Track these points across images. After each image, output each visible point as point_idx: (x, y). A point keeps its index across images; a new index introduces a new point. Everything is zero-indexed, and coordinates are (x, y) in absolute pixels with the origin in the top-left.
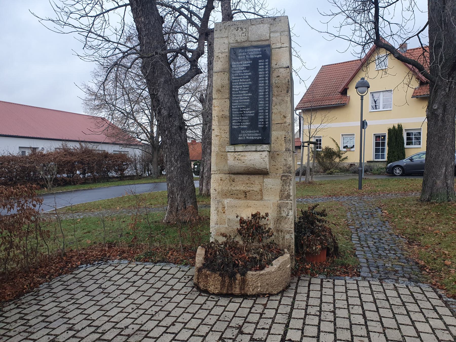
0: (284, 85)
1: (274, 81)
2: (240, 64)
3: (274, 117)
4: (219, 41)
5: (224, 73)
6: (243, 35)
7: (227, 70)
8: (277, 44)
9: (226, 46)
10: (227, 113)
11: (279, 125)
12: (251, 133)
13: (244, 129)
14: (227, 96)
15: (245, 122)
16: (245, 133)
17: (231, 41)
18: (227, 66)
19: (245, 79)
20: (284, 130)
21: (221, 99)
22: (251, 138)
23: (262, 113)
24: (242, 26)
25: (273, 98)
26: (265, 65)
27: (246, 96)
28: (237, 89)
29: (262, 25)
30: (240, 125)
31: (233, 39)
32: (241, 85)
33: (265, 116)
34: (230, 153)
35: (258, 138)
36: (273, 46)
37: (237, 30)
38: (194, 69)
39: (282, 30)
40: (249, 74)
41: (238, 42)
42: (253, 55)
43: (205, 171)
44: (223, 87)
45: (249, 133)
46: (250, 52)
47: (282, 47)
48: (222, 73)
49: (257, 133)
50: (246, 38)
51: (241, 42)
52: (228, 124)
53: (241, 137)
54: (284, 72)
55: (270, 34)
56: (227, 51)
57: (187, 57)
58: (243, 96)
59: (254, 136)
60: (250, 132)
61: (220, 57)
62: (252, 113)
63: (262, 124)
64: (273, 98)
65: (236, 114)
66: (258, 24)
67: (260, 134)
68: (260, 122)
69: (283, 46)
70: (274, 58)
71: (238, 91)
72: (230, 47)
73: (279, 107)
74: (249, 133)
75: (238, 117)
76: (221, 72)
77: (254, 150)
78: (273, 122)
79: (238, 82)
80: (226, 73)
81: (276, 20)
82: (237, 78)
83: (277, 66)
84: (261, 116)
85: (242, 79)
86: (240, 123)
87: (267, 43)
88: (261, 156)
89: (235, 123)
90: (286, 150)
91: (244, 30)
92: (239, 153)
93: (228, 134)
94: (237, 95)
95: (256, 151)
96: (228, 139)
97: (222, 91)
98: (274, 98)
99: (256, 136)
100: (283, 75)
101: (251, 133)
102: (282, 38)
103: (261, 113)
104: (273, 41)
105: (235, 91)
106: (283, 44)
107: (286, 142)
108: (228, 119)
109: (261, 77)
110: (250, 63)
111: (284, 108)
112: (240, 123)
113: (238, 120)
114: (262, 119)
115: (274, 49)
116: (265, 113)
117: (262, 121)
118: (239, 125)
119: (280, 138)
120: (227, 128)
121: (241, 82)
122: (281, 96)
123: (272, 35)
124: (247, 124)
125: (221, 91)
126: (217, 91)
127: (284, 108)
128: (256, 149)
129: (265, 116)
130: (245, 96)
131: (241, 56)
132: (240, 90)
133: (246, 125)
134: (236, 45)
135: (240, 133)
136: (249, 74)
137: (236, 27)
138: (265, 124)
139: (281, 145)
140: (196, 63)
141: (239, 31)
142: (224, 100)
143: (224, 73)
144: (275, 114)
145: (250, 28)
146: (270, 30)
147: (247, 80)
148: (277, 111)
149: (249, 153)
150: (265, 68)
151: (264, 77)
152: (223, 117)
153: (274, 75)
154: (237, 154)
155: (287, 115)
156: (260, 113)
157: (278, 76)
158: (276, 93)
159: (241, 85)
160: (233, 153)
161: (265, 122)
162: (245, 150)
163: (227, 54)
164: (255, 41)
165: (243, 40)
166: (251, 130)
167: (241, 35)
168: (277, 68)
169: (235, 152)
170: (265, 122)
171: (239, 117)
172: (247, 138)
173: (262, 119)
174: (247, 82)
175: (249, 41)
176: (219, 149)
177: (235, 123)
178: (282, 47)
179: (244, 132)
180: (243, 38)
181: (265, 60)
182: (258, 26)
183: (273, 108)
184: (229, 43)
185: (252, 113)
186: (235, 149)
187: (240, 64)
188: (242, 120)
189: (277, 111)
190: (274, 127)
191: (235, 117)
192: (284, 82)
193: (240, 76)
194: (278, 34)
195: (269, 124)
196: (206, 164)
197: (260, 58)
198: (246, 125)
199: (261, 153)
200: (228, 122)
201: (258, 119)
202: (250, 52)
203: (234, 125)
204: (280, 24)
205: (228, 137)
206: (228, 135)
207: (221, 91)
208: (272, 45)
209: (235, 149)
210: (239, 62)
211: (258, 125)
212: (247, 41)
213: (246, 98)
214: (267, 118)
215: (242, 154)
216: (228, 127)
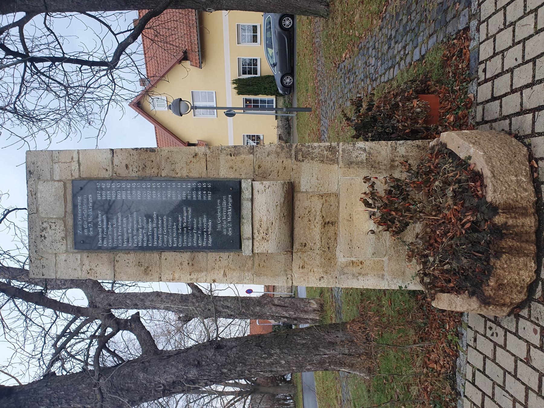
0: (142, 157)
1: (134, 175)
2: (103, 232)
3: (195, 174)
4: (62, 270)
5: (117, 261)
6: (53, 227)
7: (112, 256)
8: (73, 168)
9: (72, 257)
10: (186, 256)
12: (222, 213)
13: (214, 226)
14: (156, 255)
15: (203, 224)
16: (222, 222)
17: (64, 248)
18: (104, 256)
19: (128, 223)
20: (217, 157)
21: (160, 267)
24: (38, 229)
25: (163, 175)
27: (158, 221)
28: (145, 239)
29: (39, 195)
30: (207, 232)
31: (59, 245)
34: (255, 248)
35: (230, 200)
36: (76, 175)
37: (45, 238)
38: (131, 325)
40: (120, 216)
41: (66, 235)
42: (88, 209)
43: (287, 315)
44: (140, 264)
46: (83, 215)
49: (221, 203)
51: (66, 230)
52: (205, 254)
53: (228, 230)
54: (119, 156)
55: (55, 181)
56: (79, 256)
57: (112, 335)
58: (158, 228)
59: (227, 209)
60: (219, 214)
61: (89, 268)
62: (187, 212)
63: (207, 194)
64: (163, 175)
65: (187, 239)
66: (37, 201)
67: (224, 197)
68: (202, 197)
69: (76, 159)
70: (96, 173)
71: (148, 236)
72: (72, 250)
75: (193, 236)
76: (114, 266)
77: (250, 204)
78: (204, 175)
80: (117, 258)
81: (32, 169)
83: (110, 169)
85: (127, 230)
86: (203, 232)
87: (69, 186)
88: (260, 191)
89: (203, 241)
90: (252, 153)
91: (45, 225)
92: (255, 231)
93: (222, 254)
94: (155, 238)
95: (252, 200)
96: (232, 254)
97: (146, 265)
99: (227, 204)
100: (125, 157)
101: (222, 213)
104: (66, 176)
105: (148, 241)
106: (72, 158)
108: (196, 254)
109: (126, 195)
112: (203, 232)
113: (198, 237)
114: (197, 194)
117: (202, 193)
118: (207, 235)
119: (231, 163)
120: (212, 256)
121: (133, 230)
122: (161, 162)
123: (57, 178)
124: (205, 220)
125: (148, 267)
126: (147, 274)
130: (157, 224)
131: (89, 231)
133: (207, 222)
135: (220, 233)
136: (120, 216)
137: (39, 239)
138: (207, 189)
139: (243, 161)
140: (122, 321)
141: (46, 235)
142: (163, 261)
143: (117, 261)
144: (191, 172)
145: (43, 215)
146: (47, 181)
147: (130, 219)
149: (256, 212)
152: (192, 263)
153: (123, 172)
154: (256, 234)
157: (127, 166)
158: (155, 170)
161: (202, 189)
163: (85, 255)
164: (66, 207)
165: (62, 228)
166: (217, 212)
167: (53, 231)
168: (113, 170)
169: (253, 238)
170: (202, 189)
171: (192, 233)
172: (229, 219)
173: (197, 194)
175: (65, 216)
176: (248, 271)
177: (203, 241)
179: (219, 226)
183: (179, 175)
184: (67, 251)
185: (187, 212)
186: (248, 239)
188: (198, 229)
189: (185, 169)
190: (213, 174)
191: (192, 242)
192: (136, 157)
194: (56, 166)
196: (277, 313)
198: (207, 222)
200: (201, 256)
201: (198, 201)
202: (83, 215)
203: (207, 243)
204: (39, 163)
205: (227, 254)
206: (224, 255)
207: (148, 267)
208: (73, 178)
209: (248, 239)
210: (98, 234)
211: (207, 201)
213: (160, 222)
215: (256, 225)
216: (210, 254)
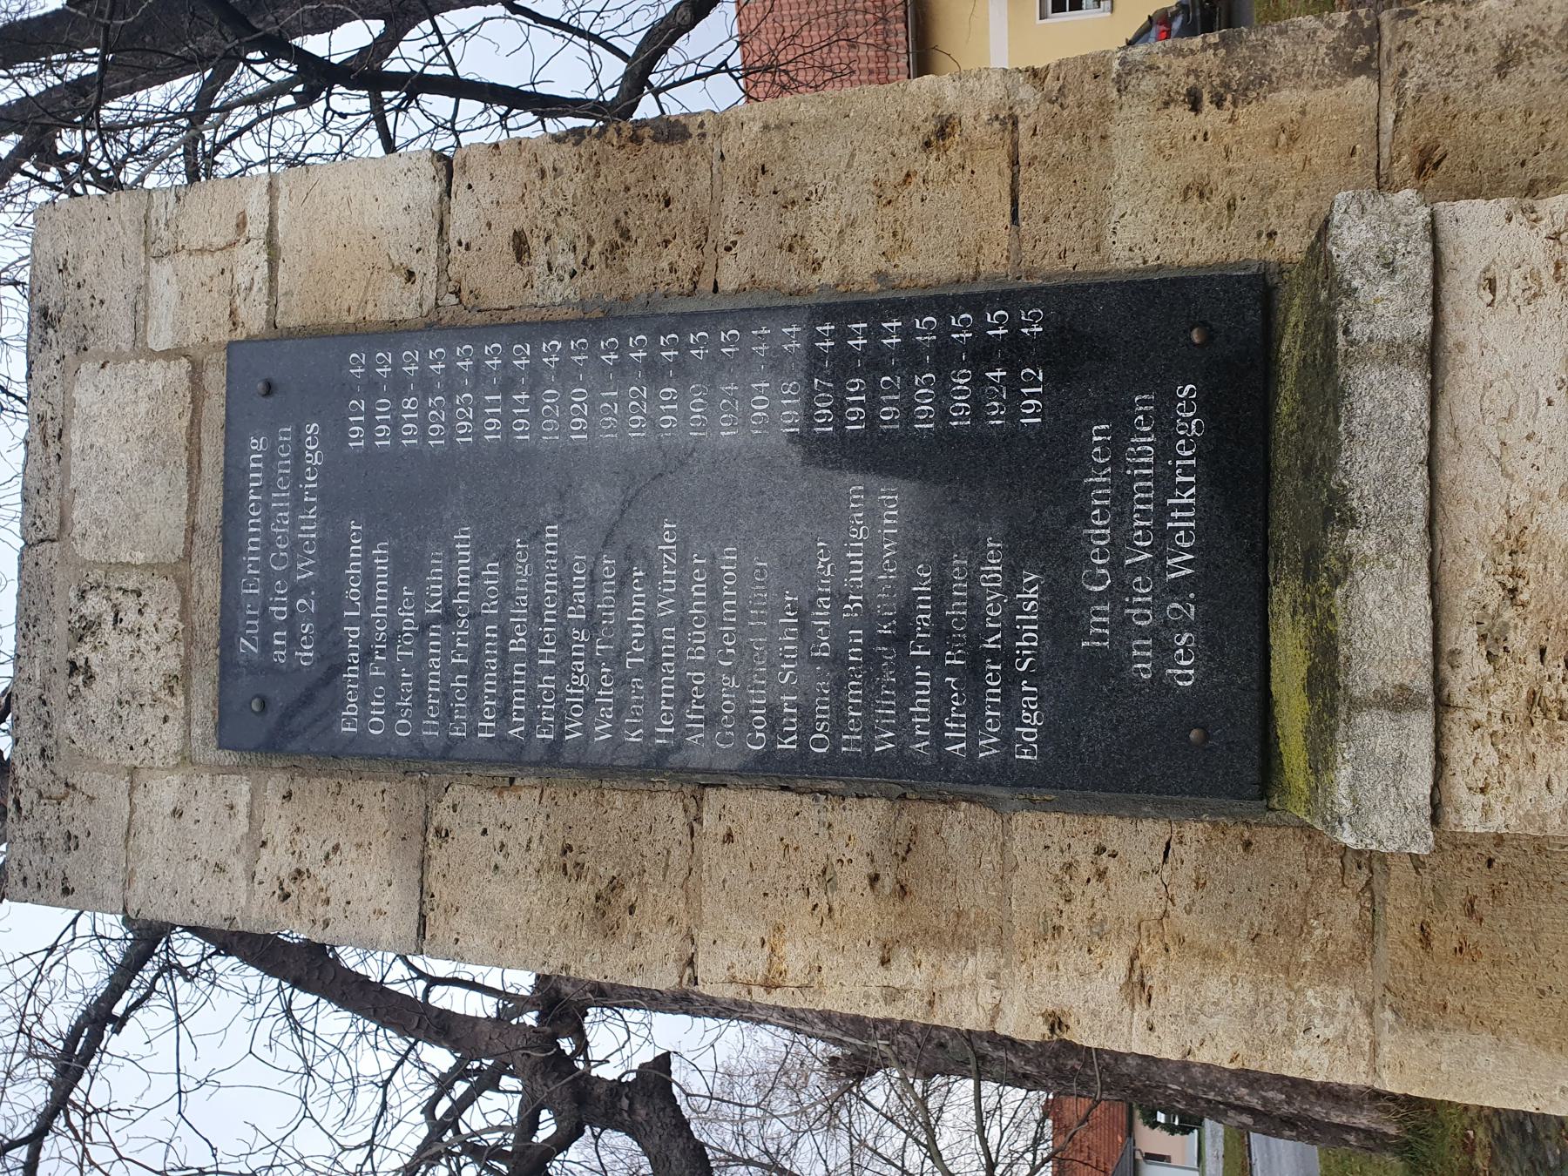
0: (611, 177)
1: (559, 291)
2: (367, 655)
3: (931, 262)
4: (158, 865)
5: (443, 834)
6: (130, 618)
7: (413, 796)
8: (242, 278)
9: (208, 795)
10: (861, 822)
11: (1037, 184)
12: (1120, 516)
13: (1063, 616)
14: (667, 807)
15: (975, 603)
16: (1120, 591)
17: (171, 736)
18: (375, 802)
19: (507, 595)
20: (1092, 131)
21: (690, 895)
22: (1182, 522)
23: (873, 391)
24: (60, 628)
25: (729, 281)
26: (399, 384)
27: (684, 582)
28: (605, 696)
29: (75, 439)
30: (1007, 656)
31: (148, 719)
32: (564, 642)
33: (910, 358)
34: (1458, 786)
35: (1190, 423)
36: (254, 319)
37: (90, 678)
38: (631, 1111)
39: (131, 240)
40: (464, 550)
41: (187, 667)
42: (298, 506)
43: (1255, 1103)
44: (568, 862)
45: (1119, 547)
46: (269, 543)
47: (271, 231)
48: (440, 858)
49: (1116, 450)
50: (162, 594)
51: (187, 636)
52: (987, 822)
53: (1164, 650)
54: (480, 188)
55: (152, 355)
56: (241, 789)
57: (562, 1142)
58: (683, 623)
59: (1165, 485)
60: (1099, 529)
61: (286, 865)
62: (873, 516)
63: (1013, 384)
64: (729, 281)
65: (867, 706)
66: (66, 472)
67: (1143, 403)
68: (978, 409)
69: (257, 228)
70: (351, 298)
71: (622, 681)
72: (213, 755)
73: (828, 206)
74: (1119, 547)
75: (905, 688)
76: (423, 864)
77: (1415, 388)
78: (994, 262)
79: (534, 672)
80: (442, 816)
81: (52, 298)
82: (490, 685)
83: (426, 266)
84: (908, 409)
85: (505, 634)
86: (976, 659)
87: (215, 378)
88: (1512, 284)
89: (975, 720)
90: (1369, 66)
91: (95, 604)
92: (1464, 638)
93: (1113, 830)
94: (667, 690)
95: (1433, 356)
96: (1193, 831)
97: (608, 869)
98: (730, 278)
99: (1165, 451)
100: (511, 192)
101: (1120, 516)
102: (196, 243)
103: (872, 406)
104: (207, 326)
105: (621, 707)
106: (241, 225)
107: (1259, 83)
108: (928, 816)
109: (507, 419)
110: (369, 543)
111: (837, 150)
112: (976, 659)
113: (941, 694)
114: (943, 391)
115: (273, 306)
116: (875, 362)
117: (978, 381)
118: (1010, 680)
119: (1195, 162)
120: (1042, 837)
121: (535, 640)
122: (717, 199)
123: (161, 337)
124: (993, 569)
125: (615, 885)
126: (611, 932)
127: (837, 150)
128: (1393, 353)
129: (910, 358)
130: (683, 602)
131: (293, 640)
132: (618, 658)
133: (1012, 584)
134: (205, 689)
135: (1110, 665)
136: (464, 550)
137: (61, 682)
138: (1014, 351)
139: (1289, 135)
140: (599, 1090)
141: (95, 659)
142: (711, 850)
143: (443, 834)
144: (903, 245)
145: (87, 551)
146: (119, 357)
147: (523, 571)
148: (867, 232)
149: (1468, 472)
150: (425, 385)
151: (508, 385)
152: (899, 877)
153: (497, 283)
154: (1472, 663)
155: (923, 112)
156: (872, 420)
157: (520, 245)
158: (683, 256)
159: (564, 642)
160: (1463, 745)
161: (982, 353)
162: (1414, 533)
163: (276, 784)
164: (193, 498)
165: (170, 622)
166: (1084, 516)
167: (129, 641)
168: (442, 270)
169: (1442, 704)
170: (982, 353)
171: (904, 667)
172: (1180, 566)
173: (943, 391)
174: (537, 571)
175: (188, 556)
176: (1330, 970)
177: (975, 720)
178: (271, 231)
179: (1099, 620)
180: (158, 617)
181: (347, 388)
182: (77, 477)
183: (829, 274)
184: (186, 758)
185: (873, 516)
186: (1399, 702)
187: (367, 655)
188: (942, 633)
189: (867, 232)
190: (1058, 250)
191: (903, 725)
192: (573, 185)
193: (476, 655)
194: (162, 273)
195: (1010, 298)
196: (1212, 1087)
197: (335, 435)
198: (1012, 584)
199: (1464, 293)
200: (960, 829)
201: (945, 437)
202: (269, 543)
203: (1007, 739)
204: (88, 266)
205: (1153, 830)
206: (1136, 838)
207: (615, 885)
208: (240, 334)
209: (1399, 702)
210: (343, 667)
211: (1013, 433)
212: (179, 572)
213: (698, 589)
214: (945, 330)
215: (1474, 584)
216: (1024, 820)
